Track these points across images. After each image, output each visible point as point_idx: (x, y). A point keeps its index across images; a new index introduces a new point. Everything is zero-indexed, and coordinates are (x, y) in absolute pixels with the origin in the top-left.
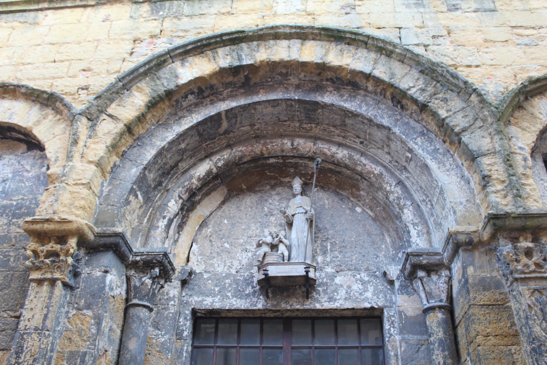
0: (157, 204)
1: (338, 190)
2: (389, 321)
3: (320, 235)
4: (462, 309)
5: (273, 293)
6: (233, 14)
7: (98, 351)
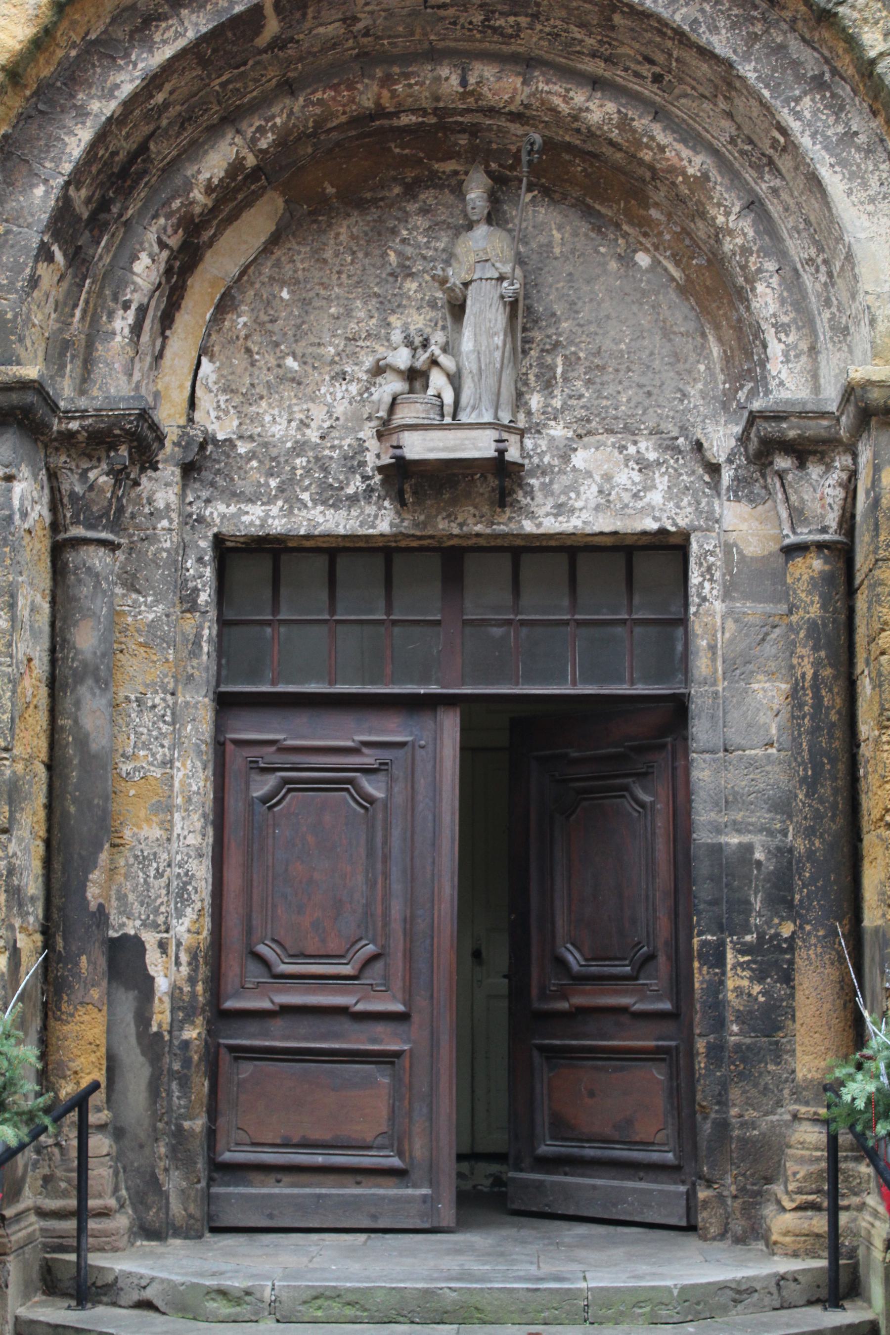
0: (101, 264)
1: (589, 200)
2: (701, 564)
3: (537, 335)
4: (867, 556)
5: (415, 493)
7: (17, 667)
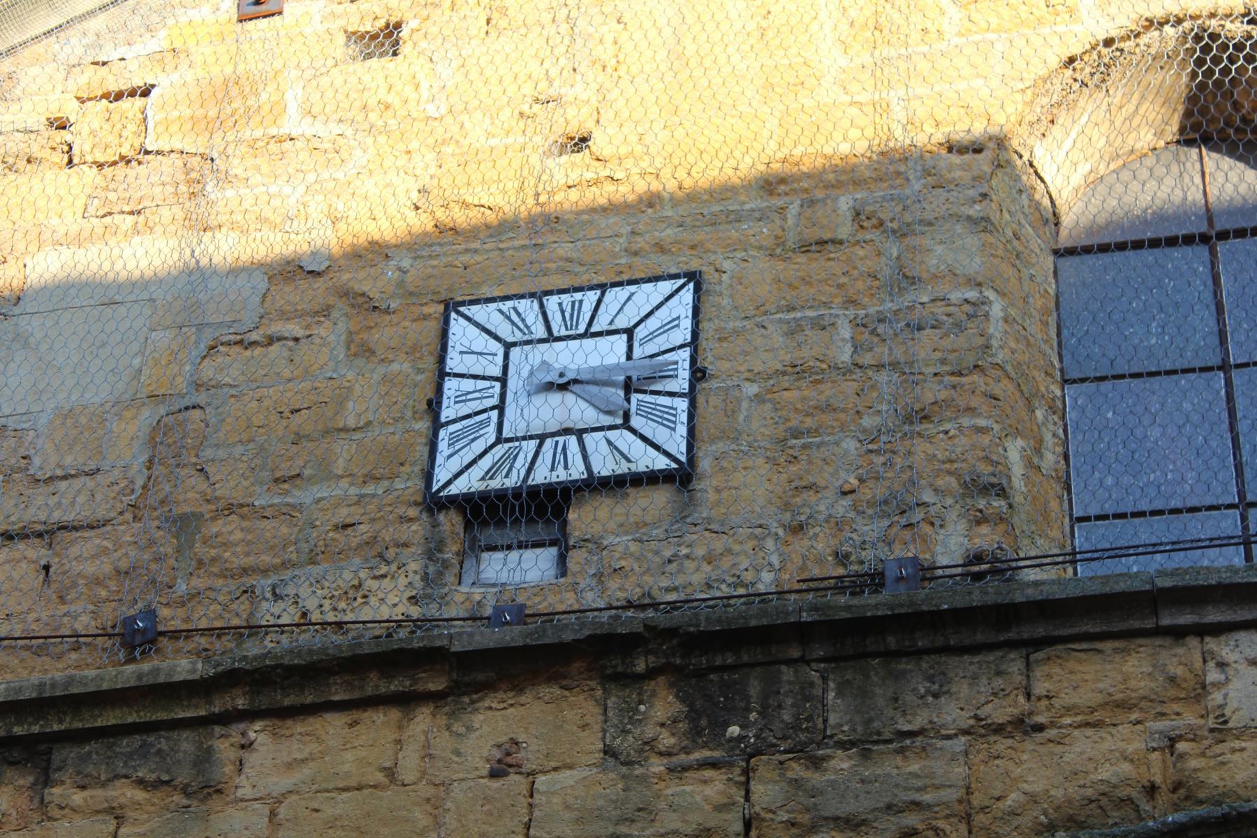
6: (1040, 728)
